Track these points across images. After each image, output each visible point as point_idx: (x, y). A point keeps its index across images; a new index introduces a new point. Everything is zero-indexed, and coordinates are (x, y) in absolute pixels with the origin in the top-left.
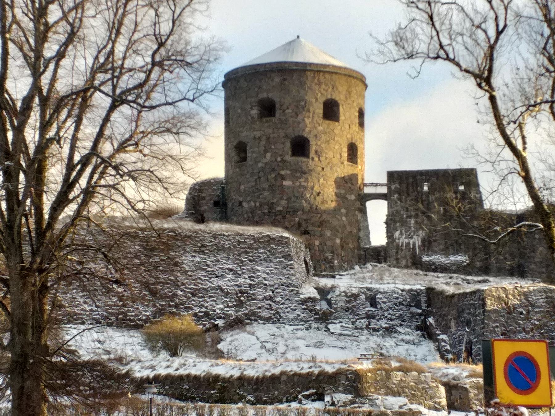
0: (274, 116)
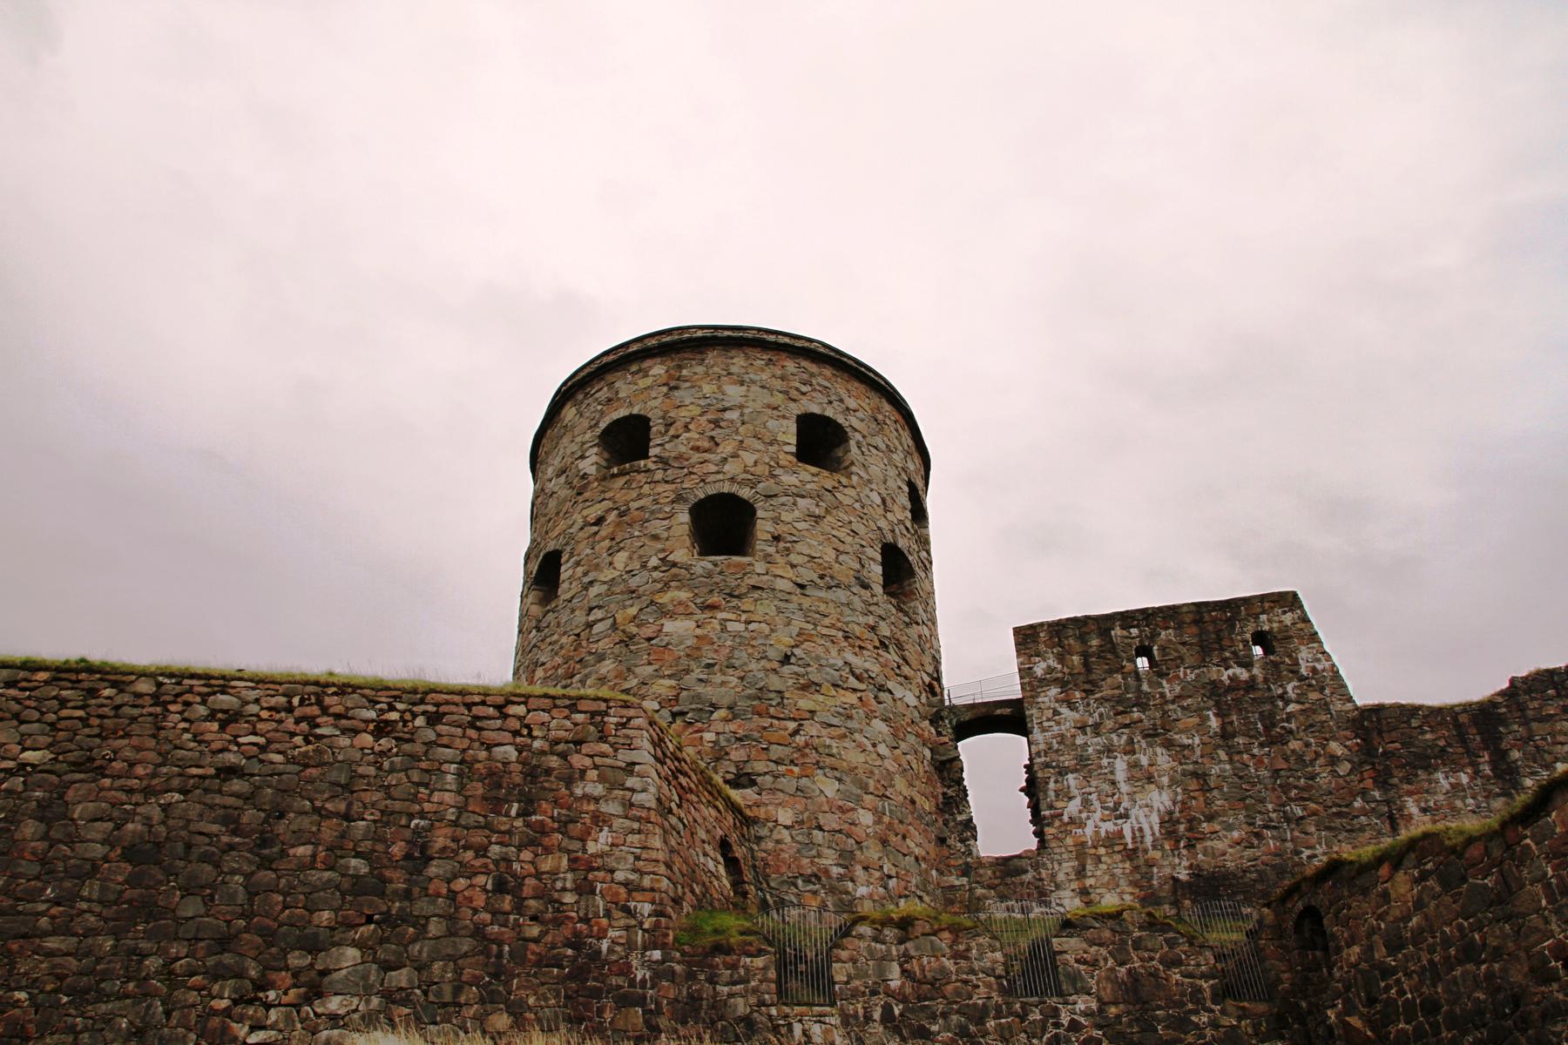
0: (647, 457)
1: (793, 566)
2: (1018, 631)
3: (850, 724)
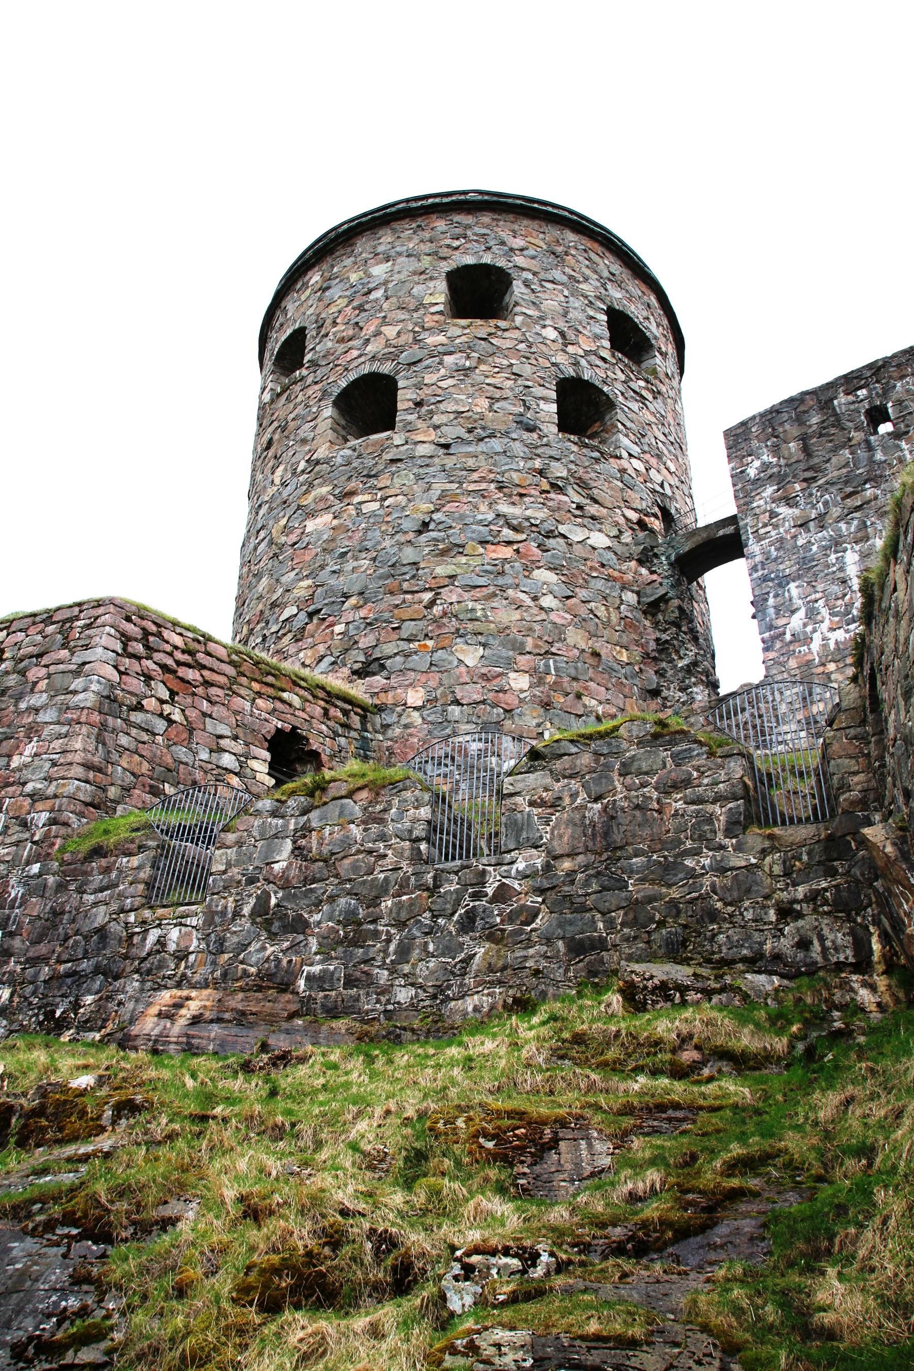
1: (436, 427)
2: (728, 434)
3: (500, 581)
